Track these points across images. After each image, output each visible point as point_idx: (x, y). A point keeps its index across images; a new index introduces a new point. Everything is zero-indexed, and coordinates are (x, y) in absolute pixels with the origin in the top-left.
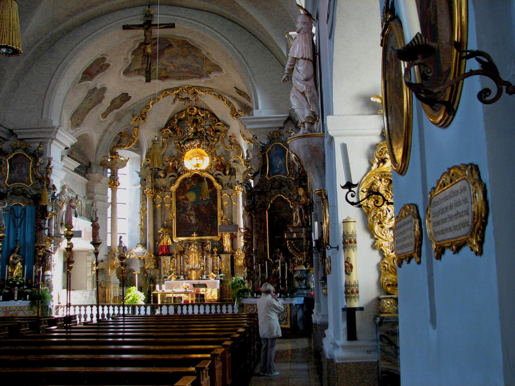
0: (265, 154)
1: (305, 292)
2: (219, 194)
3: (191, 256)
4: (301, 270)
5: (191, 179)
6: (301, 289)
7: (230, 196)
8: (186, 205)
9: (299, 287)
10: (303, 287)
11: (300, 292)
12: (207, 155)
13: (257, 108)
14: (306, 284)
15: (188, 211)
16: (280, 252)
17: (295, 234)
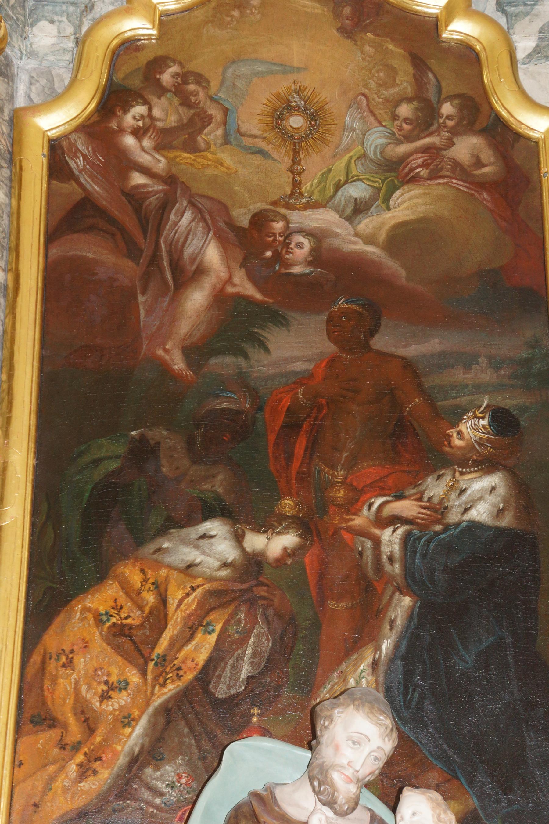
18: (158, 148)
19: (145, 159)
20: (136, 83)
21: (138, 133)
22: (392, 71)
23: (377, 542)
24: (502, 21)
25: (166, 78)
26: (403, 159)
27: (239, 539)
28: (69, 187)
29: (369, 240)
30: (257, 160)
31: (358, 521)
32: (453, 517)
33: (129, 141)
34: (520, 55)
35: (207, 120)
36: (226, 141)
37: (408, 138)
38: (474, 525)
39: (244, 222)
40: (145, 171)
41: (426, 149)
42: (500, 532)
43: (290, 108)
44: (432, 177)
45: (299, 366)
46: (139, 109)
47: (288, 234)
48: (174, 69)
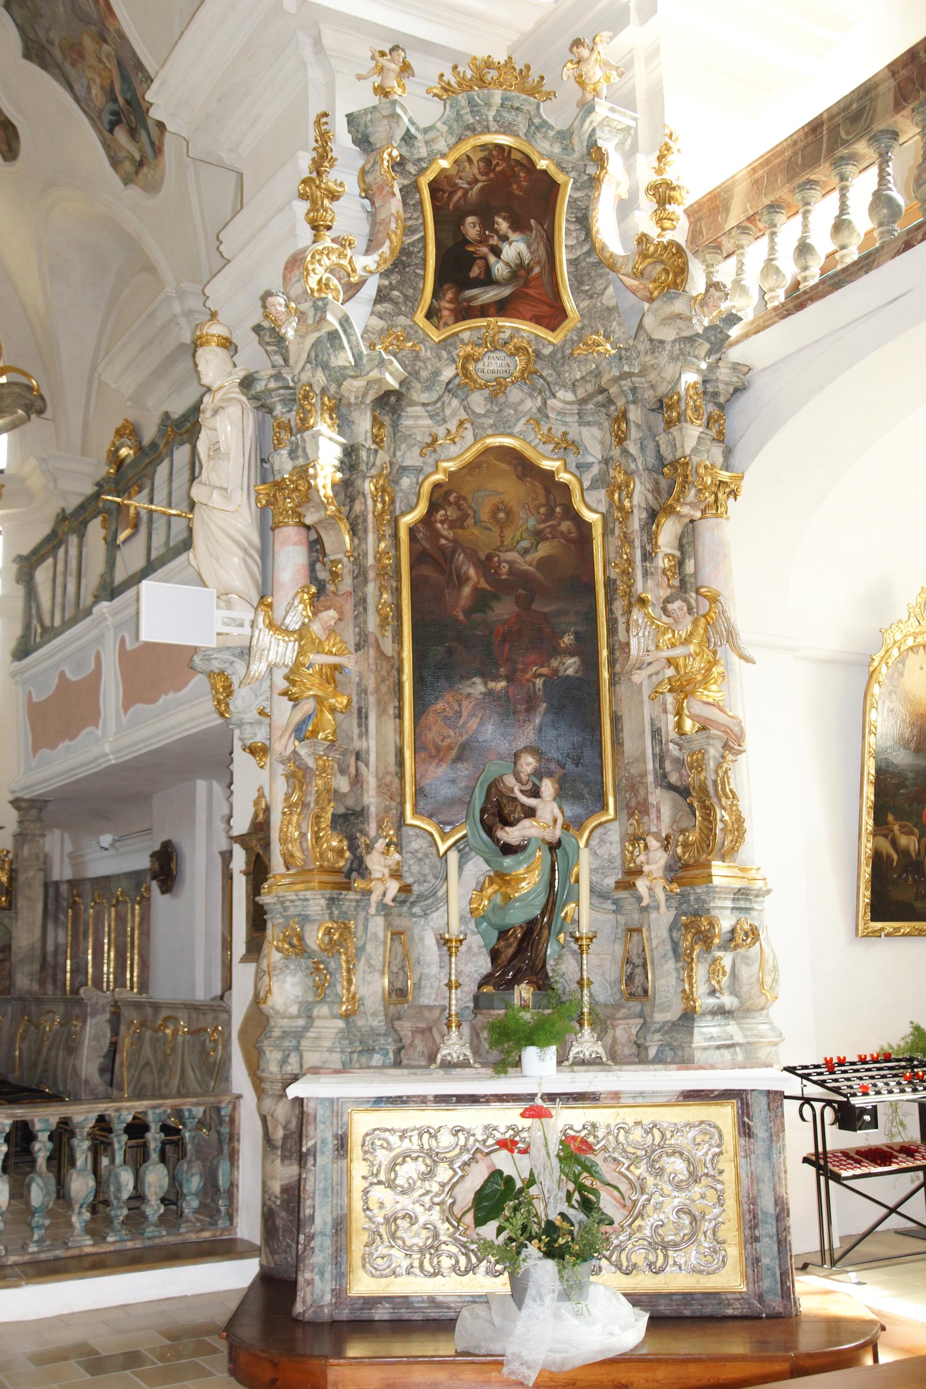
0: (416, 187)
16: (539, 774)
18: (450, 528)
19: (445, 533)
20: (440, 501)
21: (442, 522)
22: (536, 493)
23: (534, 684)
24: (577, 473)
25: (452, 498)
26: (542, 531)
27: (486, 684)
28: (418, 546)
29: (530, 564)
30: (487, 532)
31: (528, 676)
32: (561, 674)
33: (439, 525)
34: (585, 487)
35: (468, 515)
36: (475, 524)
37: (544, 522)
38: (568, 676)
39: (483, 558)
40: (445, 538)
41: (550, 526)
42: (578, 679)
43: (499, 510)
44: (554, 537)
45: (505, 617)
46: (442, 512)
47: (500, 562)
48: (454, 495)
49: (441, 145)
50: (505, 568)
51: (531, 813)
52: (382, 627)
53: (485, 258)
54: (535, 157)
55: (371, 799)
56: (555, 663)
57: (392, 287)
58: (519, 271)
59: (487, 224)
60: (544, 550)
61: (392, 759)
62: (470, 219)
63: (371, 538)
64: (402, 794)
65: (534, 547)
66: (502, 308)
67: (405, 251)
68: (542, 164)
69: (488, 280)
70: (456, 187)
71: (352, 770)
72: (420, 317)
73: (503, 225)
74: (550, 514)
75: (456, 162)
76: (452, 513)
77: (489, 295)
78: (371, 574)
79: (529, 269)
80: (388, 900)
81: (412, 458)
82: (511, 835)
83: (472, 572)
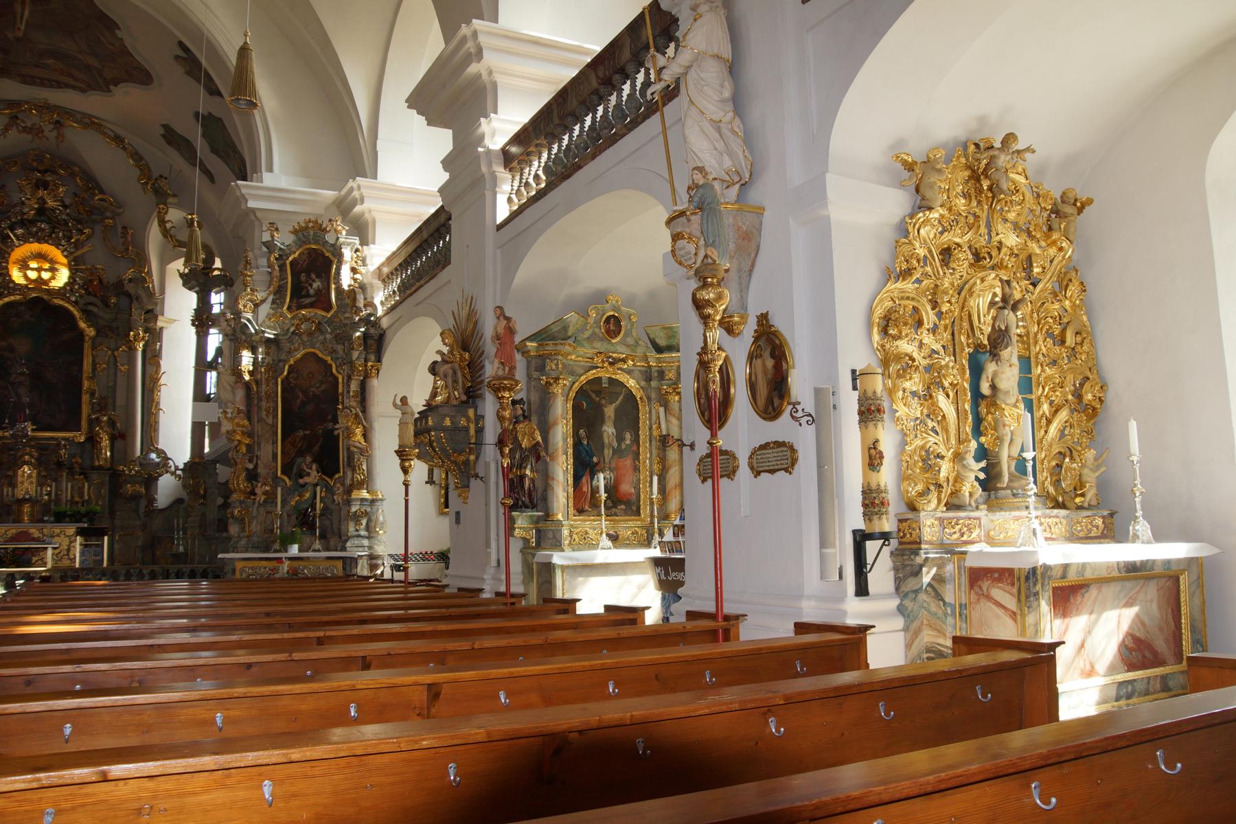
0: (285, 264)
1: (366, 542)
2: (87, 346)
3: (20, 472)
4: (363, 500)
5: (23, 308)
6: (359, 536)
7: (113, 351)
8: (9, 363)
9: (356, 533)
10: (363, 533)
11: (357, 542)
12: (65, 261)
13: (270, 169)
14: (368, 528)
15: (14, 376)
17: (448, 419)
49: (294, 249)
50: (311, 393)
51: (308, 474)
52: (267, 416)
53: (307, 288)
54: (325, 251)
55: (261, 471)
56: (325, 425)
57: (277, 299)
58: (318, 292)
59: (308, 276)
60: (323, 387)
61: (271, 457)
62: (303, 274)
63: (264, 386)
64: (277, 468)
65: (320, 386)
66: (312, 305)
67: (279, 287)
68: (327, 254)
69: (308, 296)
70: (298, 263)
71: (255, 461)
72: (285, 308)
73: (313, 276)
74: (326, 375)
75: (299, 255)
76: (295, 375)
77: (308, 301)
78: (264, 398)
79: (321, 291)
80: (261, 502)
81: (283, 357)
82: (301, 481)
83: (300, 395)
